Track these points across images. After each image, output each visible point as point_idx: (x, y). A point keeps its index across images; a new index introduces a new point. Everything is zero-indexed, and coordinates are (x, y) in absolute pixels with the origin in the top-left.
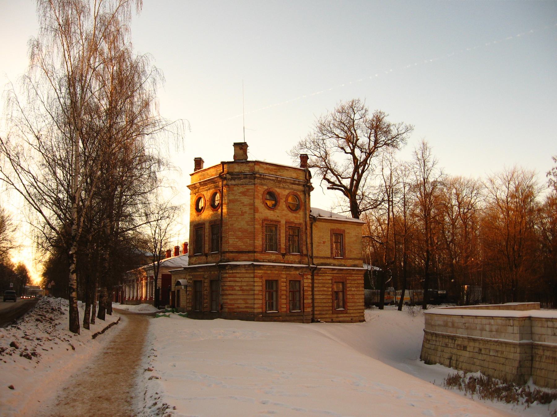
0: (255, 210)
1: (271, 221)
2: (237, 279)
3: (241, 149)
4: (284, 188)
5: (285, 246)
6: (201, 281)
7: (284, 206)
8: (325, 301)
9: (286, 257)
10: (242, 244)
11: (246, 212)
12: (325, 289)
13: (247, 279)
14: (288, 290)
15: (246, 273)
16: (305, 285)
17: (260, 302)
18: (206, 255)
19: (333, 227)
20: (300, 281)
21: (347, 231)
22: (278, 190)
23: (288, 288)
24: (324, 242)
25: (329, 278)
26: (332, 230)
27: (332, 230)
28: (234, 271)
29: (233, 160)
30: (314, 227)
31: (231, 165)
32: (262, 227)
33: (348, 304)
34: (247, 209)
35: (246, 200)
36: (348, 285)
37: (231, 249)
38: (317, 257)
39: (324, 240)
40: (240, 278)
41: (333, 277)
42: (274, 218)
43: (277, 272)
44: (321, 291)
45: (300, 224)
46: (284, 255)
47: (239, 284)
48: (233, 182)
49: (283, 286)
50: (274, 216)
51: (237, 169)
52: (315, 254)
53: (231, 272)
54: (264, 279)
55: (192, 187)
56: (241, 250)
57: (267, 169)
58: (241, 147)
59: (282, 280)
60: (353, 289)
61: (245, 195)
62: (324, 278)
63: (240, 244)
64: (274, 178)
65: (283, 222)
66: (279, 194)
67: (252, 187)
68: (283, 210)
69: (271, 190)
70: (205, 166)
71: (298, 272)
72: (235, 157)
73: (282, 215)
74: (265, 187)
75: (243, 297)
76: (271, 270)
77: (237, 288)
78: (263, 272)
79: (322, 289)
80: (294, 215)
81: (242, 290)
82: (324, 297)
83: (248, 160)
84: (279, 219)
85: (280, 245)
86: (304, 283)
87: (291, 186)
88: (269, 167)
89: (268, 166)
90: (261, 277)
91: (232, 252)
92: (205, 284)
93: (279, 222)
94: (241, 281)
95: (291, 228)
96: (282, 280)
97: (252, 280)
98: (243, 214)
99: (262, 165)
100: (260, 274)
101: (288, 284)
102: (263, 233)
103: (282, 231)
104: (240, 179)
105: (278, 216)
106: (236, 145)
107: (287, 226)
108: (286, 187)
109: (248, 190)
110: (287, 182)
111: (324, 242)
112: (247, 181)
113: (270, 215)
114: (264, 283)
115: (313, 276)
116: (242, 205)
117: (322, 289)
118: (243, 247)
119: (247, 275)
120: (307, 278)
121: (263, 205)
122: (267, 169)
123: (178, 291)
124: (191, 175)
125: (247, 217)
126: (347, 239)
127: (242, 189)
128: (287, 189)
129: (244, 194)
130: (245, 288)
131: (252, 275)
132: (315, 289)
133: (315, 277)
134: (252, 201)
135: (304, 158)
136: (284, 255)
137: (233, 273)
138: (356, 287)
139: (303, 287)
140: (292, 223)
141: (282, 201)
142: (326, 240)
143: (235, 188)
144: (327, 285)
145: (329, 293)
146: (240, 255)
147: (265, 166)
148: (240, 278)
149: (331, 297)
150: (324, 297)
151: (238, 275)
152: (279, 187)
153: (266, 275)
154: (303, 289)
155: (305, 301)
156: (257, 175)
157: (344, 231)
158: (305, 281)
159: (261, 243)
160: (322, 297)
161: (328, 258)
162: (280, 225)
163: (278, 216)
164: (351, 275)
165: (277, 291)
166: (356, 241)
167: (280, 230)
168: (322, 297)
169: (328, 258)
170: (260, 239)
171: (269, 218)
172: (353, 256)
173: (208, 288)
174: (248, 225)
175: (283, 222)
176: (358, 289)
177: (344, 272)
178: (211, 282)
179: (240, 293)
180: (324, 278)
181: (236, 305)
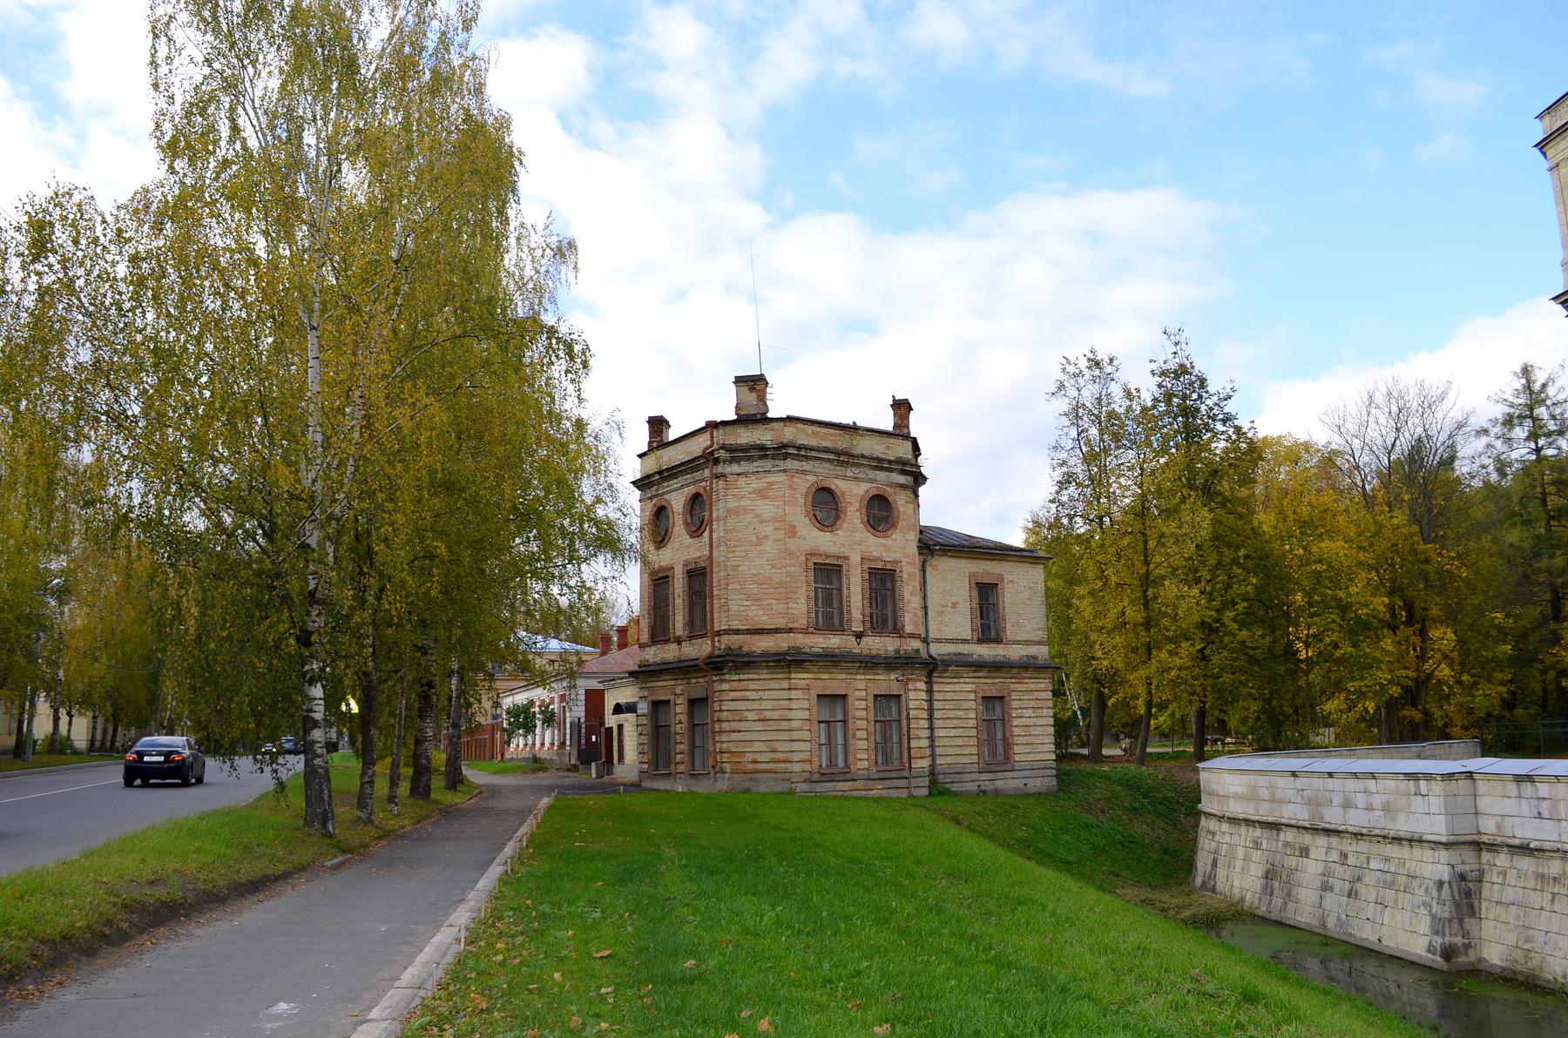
0: (792, 532)
3: (752, 389)
6: (668, 702)
7: (857, 521)
8: (960, 742)
11: (766, 537)
13: (775, 694)
14: (872, 718)
16: (912, 704)
17: (807, 747)
18: (679, 641)
20: (899, 696)
21: (1007, 577)
24: (955, 605)
26: (972, 575)
27: (972, 575)
29: (733, 417)
30: (928, 569)
31: (728, 429)
32: (807, 570)
33: (1016, 749)
34: (769, 529)
35: (766, 509)
36: (1015, 704)
37: (735, 625)
38: (939, 641)
39: (954, 599)
42: (834, 550)
45: (897, 562)
47: (755, 705)
48: (735, 468)
49: (860, 709)
51: (745, 436)
53: (736, 677)
54: (814, 693)
55: (640, 484)
58: (753, 384)
59: (857, 694)
60: (1027, 713)
61: (764, 498)
62: (957, 688)
65: (855, 558)
66: (844, 493)
67: (781, 477)
70: (673, 434)
71: (893, 677)
72: (737, 408)
73: (852, 542)
74: (812, 478)
75: (764, 737)
77: (751, 716)
79: (952, 714)
83: (770, 415)
84: (845, 551)
85: (849, 612)
86: (908, 700)
87: (871, 474)
89: (815, 428)
91: (737, 632)
92: (679, 709)
95: (873, 572)
96: (857, 694)
97: (785, 695)
98: (761, 540)
103: (852, 579)
104: (751, 459)
106: (739, 381)
111: (955, 605)
112: (766, 464)
113: (826, 542)
114: (815, 701)
115: (929, 683)
117: (952, 714)
119: (773, 685)
123: (620, 727)
124: (640, 456)
125: (770, 548)
126: (1007, 595)
127: (755, 483)
128: (862, 480)
129: (760, 494)
130: (768, 714)
132: (937, 715)
133: (936, 687)
135: (902, 408)
136: (859, 636)
140: (876, 559)
142: (960, 600)
143: (742, 481)
144: (965, 705)
145: (972, 723)
147: (809, 429)
149: (974, 732)
151: (751, 685)
152: (844, 478)
153: (818, 683)
156: (791, 451)
157: (1001, 577)
158: (912, 695)
160: (953, 733)
161: (965, 641)
165: (844, 722)
168: (953, 733)
169: (965, 641)
170: (803, 600)
171: (823, 549)
173: (684, 718)
174: (774, 566)
175: (855, 558)
178: (692, 703)
179: (759, 726)
180: (957, 688)
181: (749, 757)
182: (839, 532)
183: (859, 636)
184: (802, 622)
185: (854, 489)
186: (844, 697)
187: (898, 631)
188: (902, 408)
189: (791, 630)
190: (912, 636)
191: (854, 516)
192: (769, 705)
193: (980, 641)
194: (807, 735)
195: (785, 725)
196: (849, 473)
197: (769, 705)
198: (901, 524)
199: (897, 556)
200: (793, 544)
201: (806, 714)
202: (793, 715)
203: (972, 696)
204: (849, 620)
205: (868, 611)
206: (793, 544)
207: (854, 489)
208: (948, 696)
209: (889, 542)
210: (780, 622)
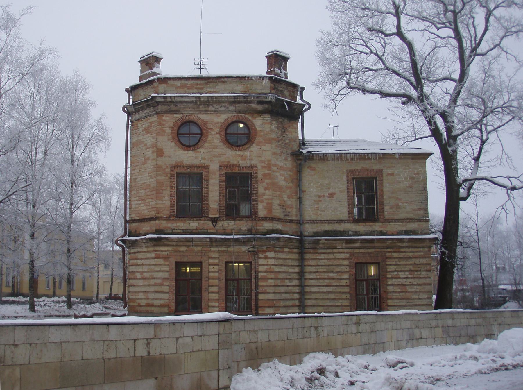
0: (160, 153)
1: (189, 167)
2: (139, 262)
4: (216, 112)
5: (220, 205)
8: (332, 296)
9: (220, 224)
10: (145, 208)
11: (148, 158)
12: (331, 275)
15: (148, 251)
16: (260, 268)
17: (166, 296)
19: (353, 167)
21: (386, 171)
22: (204, 117)
23: (224, 273)
24: (331, 195)
25: (343, 256)
28: (136, 250)
32: (172, 177)
36: (391, 268)
39: (331, 191)
40: (141, 259)
41: (352, 254)
42: (196, 162)
43: (200, 248)
44: (324, 279)
45: (252, 167)
46: (214, 221)
47: (140, 269)
50: (196, 158)
52: (309, 214)
54: (173, 260)
56: (143, 217)
57: (182, 86)
60: (402, 275)
61: (148, 133)
63: (143, 207)
64: (194, 99)
66: (206, 123)
67: (155, 118)
68: (215, 147)
69: (189, 118)
71: (244, 248)
75: (144, 289)
76: (188, 246)
77: (138, 276)
78: (170, 249)
79: (325, 275)
80: (238, 153)
81: (143, 278)
82: (330, 289)
88: (186, 82)
89: (183, 82)
90: (166, 258)
93: (208, 167)
94: (143, 265)
99: (171, 82)
100: (165, 253)
101: (223, 269)
102: (171, 187)
103: (211, 182)
105: (204, 159)
107: (223, 172)
108: (222, 109)
109: (151, 123)
110: (222, 102)
113: (188, 157)
114: (174, 266)
116: (144, 148)
117: (325, 275)
118: (146, 213)
119: (148, 255)
120: (266, 258)
121: (173, 144)
122: (182, 86)
130: (146, 275)
131: (153, 255)
132: (307, 276)
134: (154, 140)
135: (277, 60)
137: (135, 253)
138: (410, 271)
139: (257, 272)
140: (233, 165)
141: (213, 133)
144: (338, 269)
146: (143, 224)
147: (178, 83)
148: (141, 259)
149: (347, 289)
150: (330, 289)
151: (140, 256)
152: (206, 112)
154: (257, 276)
155: (261, 297)
157: (381, 171)
159: (168, 203)
160: (325, 289)
162: (208, 172)
163: (204, 159)
164: (398, 249)
166: (411, 187)
167: (208, 181)
168: (325, 289)
170: (167, 198)
172: (403, 216)
175: (214, 166)
176: (417, 274)
177: (376, 244)
179: (141, 282)
180: (331, 256)
182: (202, 150)
183: (214, 221)
184: (166, 213)
185: (214, 120)
186: (201, 262)
187: (253, 216)
188: (277, 60)
189: (156, 218)
190: (265, 219)
191: (214, 138)
192: (145, 269)
193: (356, 221)
194: (166, 289)
195: (152, 282)
196: (211, 108)
197: (145, 269)
198: (258, 139)
199: (254, 163)
200: (161, 161)
201: (166, 275)
202: (156, 275)
203: (346, 262)
204: (207, 210)
205: (223, 203)
206: (161, 161)
207: (214, 120)
208: (322, 263)
209: (247, 153)
210: (153, 213)
